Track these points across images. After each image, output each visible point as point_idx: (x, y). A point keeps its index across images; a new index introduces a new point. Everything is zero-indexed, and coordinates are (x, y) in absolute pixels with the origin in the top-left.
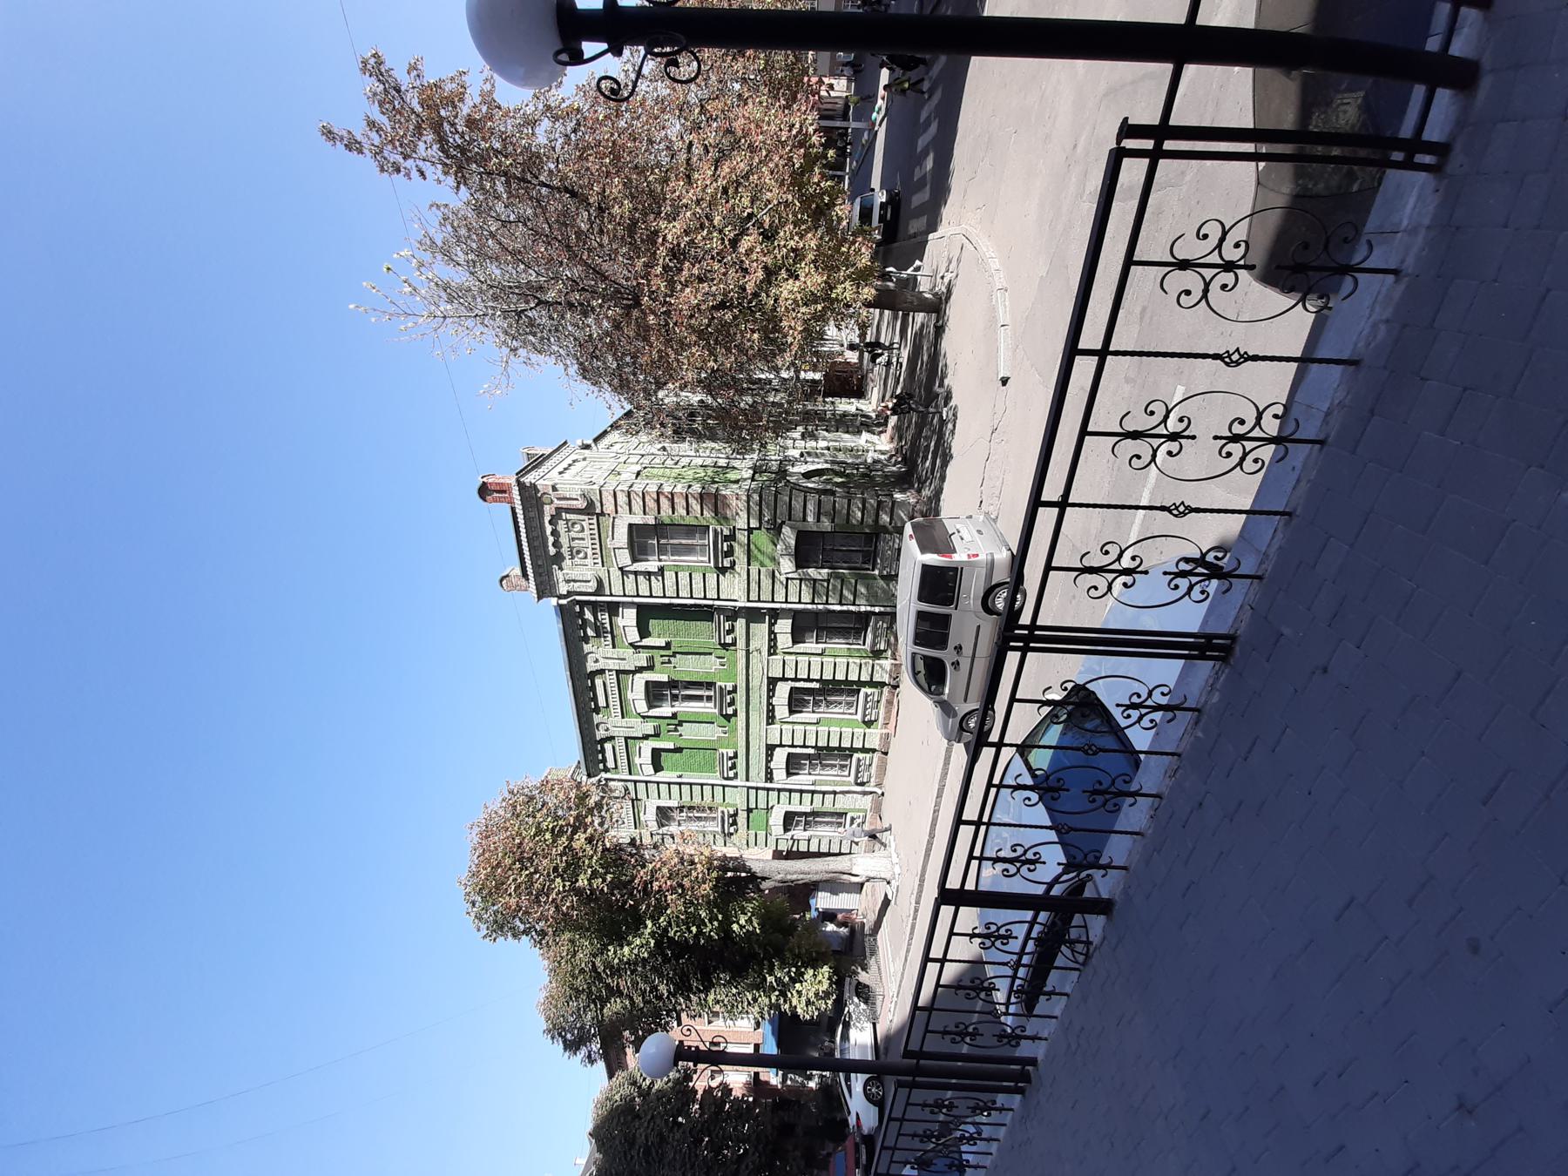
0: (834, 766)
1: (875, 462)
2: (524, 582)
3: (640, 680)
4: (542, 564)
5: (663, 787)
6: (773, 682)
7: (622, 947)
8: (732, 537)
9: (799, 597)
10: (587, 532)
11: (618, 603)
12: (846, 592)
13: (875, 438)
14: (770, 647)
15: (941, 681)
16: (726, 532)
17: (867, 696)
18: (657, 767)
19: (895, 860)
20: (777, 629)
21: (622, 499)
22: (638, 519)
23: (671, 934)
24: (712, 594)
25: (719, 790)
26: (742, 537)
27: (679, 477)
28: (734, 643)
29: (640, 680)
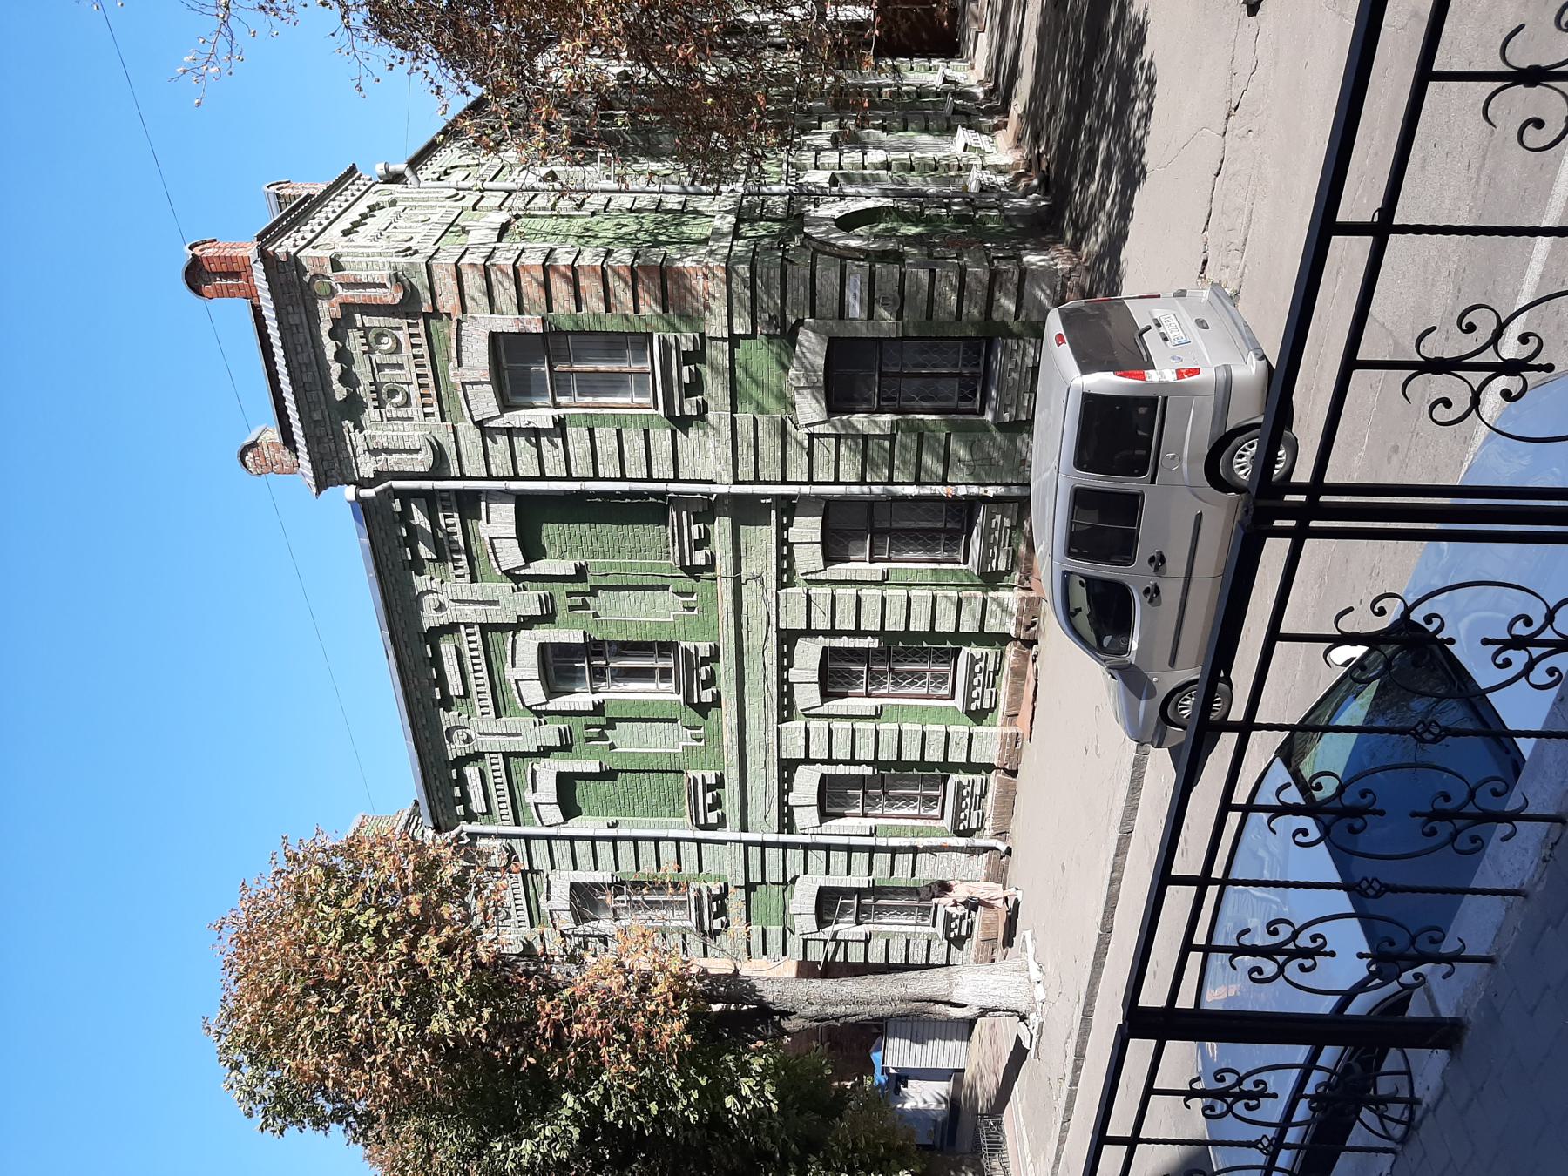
0: (909, 799)
1: (984, 189)
2: (288, 457)
3: (528, 643)
4: (320, 420)
5: (582, 848)
6: (788, 639)
7: (518, 1140)
8: (696, 356)
9: (838, 473)
10: (407, 352)
11: (476, 495)
12: (928, 460)
13: (983, 141)
14: (780, 572)
15: (1123, 626)
16: (687, 345)
17: (972, 661)
18: (569, 808)
19: (1035, 974)
20: (793, 534)
21: (473, 282)
22: (507, 323)
23: (609, 1116)
24: (663, 469)
25: (689, 850)
26: (719, 354)
27: (586, 235)
28: (710, 565)
29: (528, 643)
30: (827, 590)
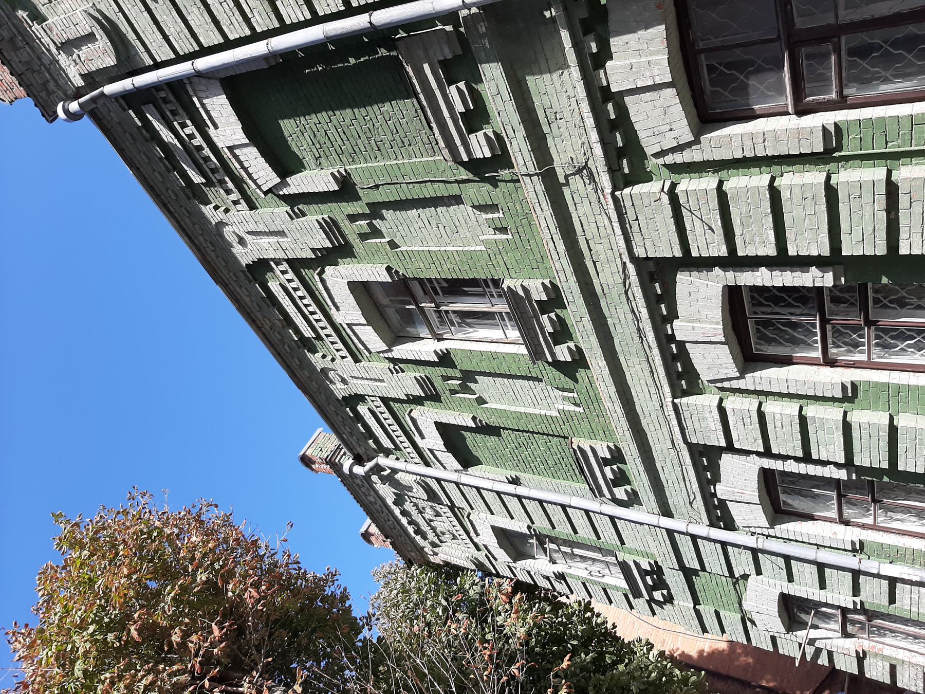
11: (176, 86)
14: (613, 157)
20: (618, 74)
28: (501, 157)
30: (709, 182)
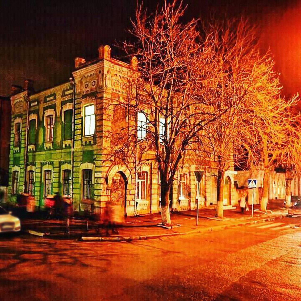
6: (52, 164)
14: (62, 162)
